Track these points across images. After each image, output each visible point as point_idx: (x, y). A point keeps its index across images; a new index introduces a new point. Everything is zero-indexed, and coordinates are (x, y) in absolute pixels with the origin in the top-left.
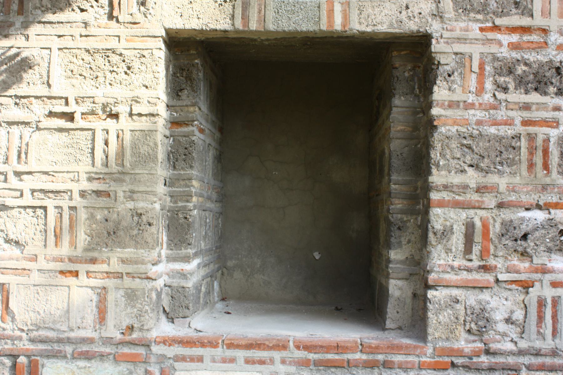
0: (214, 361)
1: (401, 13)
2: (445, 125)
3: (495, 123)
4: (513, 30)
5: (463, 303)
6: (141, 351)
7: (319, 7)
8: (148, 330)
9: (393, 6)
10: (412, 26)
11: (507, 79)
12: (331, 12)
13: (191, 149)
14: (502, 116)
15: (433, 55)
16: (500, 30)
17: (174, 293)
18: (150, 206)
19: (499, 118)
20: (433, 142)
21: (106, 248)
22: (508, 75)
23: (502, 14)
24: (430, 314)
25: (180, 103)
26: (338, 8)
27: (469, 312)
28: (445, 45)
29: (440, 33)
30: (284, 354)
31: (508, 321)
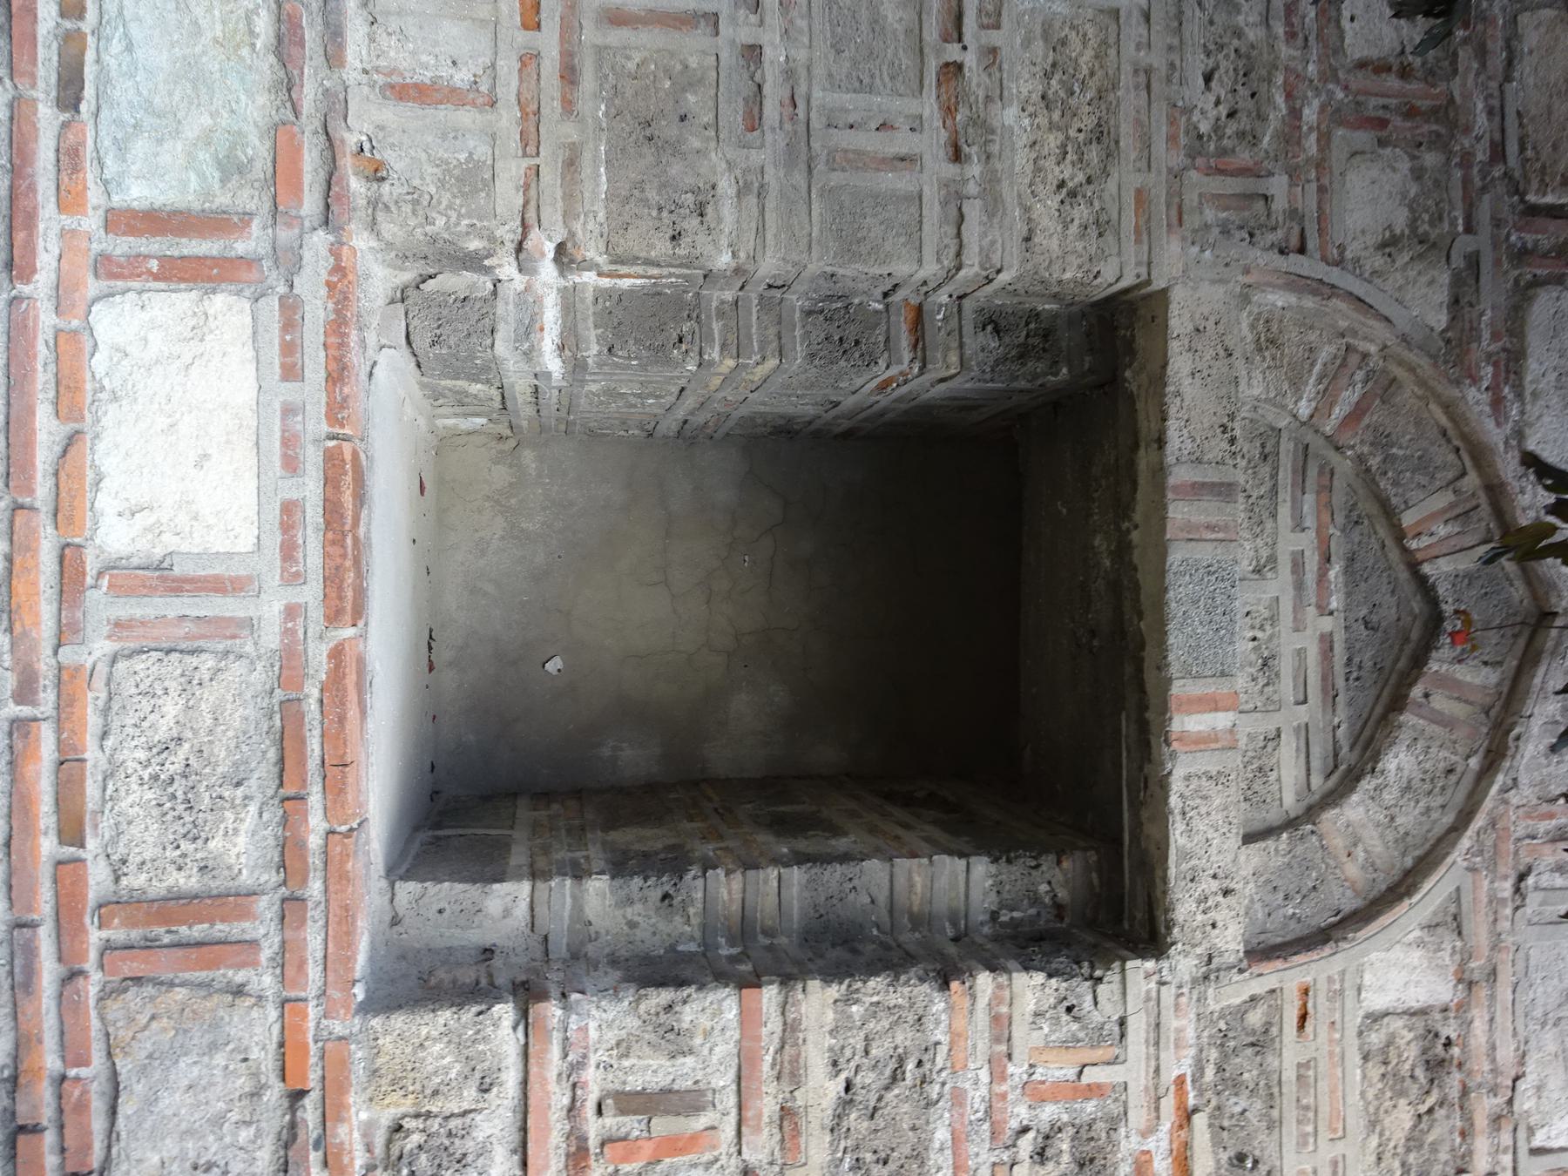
0: (288, 411)
1: (1214, 876)
2: (950, 1008)
5: (480, 1105)
6: (310, 204)
7: (1223, 674)
8: (374, 221)
9: (1230, 858)
10: (1184, 908)
11: (1066, 1158)
12: (1212, 704)
13: (857, 355)
14: (977, 1155)
15: (1116, 965)
16: (1181, 1127)
17: (478, 305)
18: (724, 242)
19: (973, 1149)
20: (906, 983)
21: (606, 114)
22: (1075, 1160)
23: (1217, 1129)
24: (446, 1015)
25: (968, 328)
26: (1222, 720)
27: (454, 1124)
28: (1143, 995)
29: (1169, 979)
30: (316, 614)
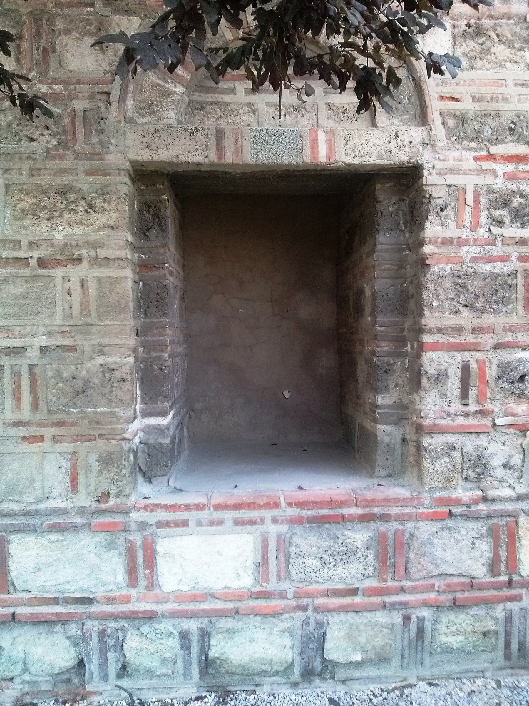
0: (199, 524)
1: (390, 142)
2: (437, 263)
3: (490, 260)
4: (508, 159)
5: (460, 450)
6: (119, 518)
7: (301, 136)
8: (125, 496)
9: (382, 134)
11: (502, 212)
12: (314, 142)
13: (163, 295)
14: (498, 252)
15: (425, 188)
16: (495, 159)
17: (151, 450)
18: (125, 361)
19: (495, 254)
20: (426, 282)
21: (76, 409)
22: (503, 207)
23: (497, 141)
24: (426, 463)
25: (147, 244)
26: (322, 137)
27: (466, 459)
28: (438, 177)
29: (432, 164)
30: (275, 512)
31: (506, 466)
